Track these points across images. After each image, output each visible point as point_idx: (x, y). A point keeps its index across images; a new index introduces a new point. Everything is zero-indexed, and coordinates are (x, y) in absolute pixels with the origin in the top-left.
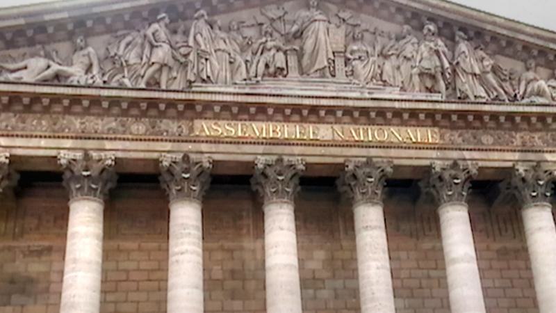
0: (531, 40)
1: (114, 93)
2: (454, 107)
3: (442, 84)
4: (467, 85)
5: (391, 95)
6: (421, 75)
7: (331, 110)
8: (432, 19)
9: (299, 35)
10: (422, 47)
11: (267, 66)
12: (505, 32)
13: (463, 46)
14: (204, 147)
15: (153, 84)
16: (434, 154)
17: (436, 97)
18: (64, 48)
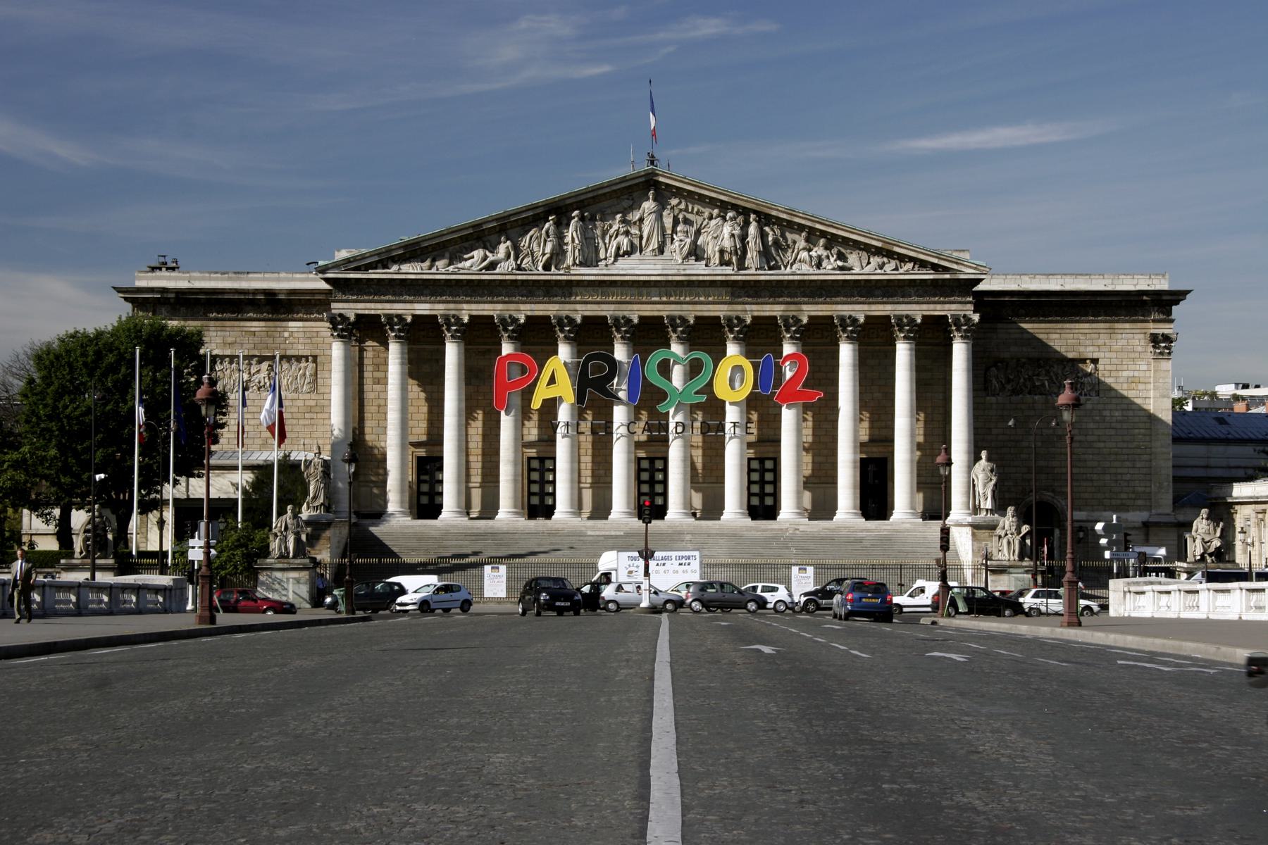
0: (803, 222)
1: (524, 278)
2: (739, 278)
3: (734, 259)
4: (752, 257)
5: (698, 270)
6: (722, 252)
7: (656, 284)
8: (735, 207)
9: (641, 220)
10: (727, 229)
11: (618, 248)
12: (785, 216)
13: (752, 229)
14: (578, 307)
15: (547, 267)
16: (725, 307)
17: (728, 270)
18: (493, 238)
